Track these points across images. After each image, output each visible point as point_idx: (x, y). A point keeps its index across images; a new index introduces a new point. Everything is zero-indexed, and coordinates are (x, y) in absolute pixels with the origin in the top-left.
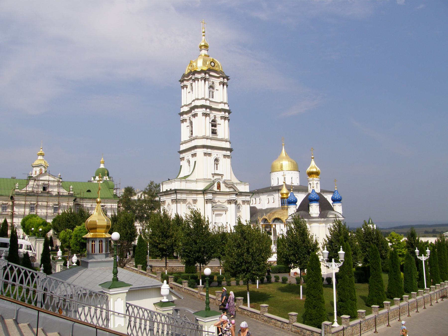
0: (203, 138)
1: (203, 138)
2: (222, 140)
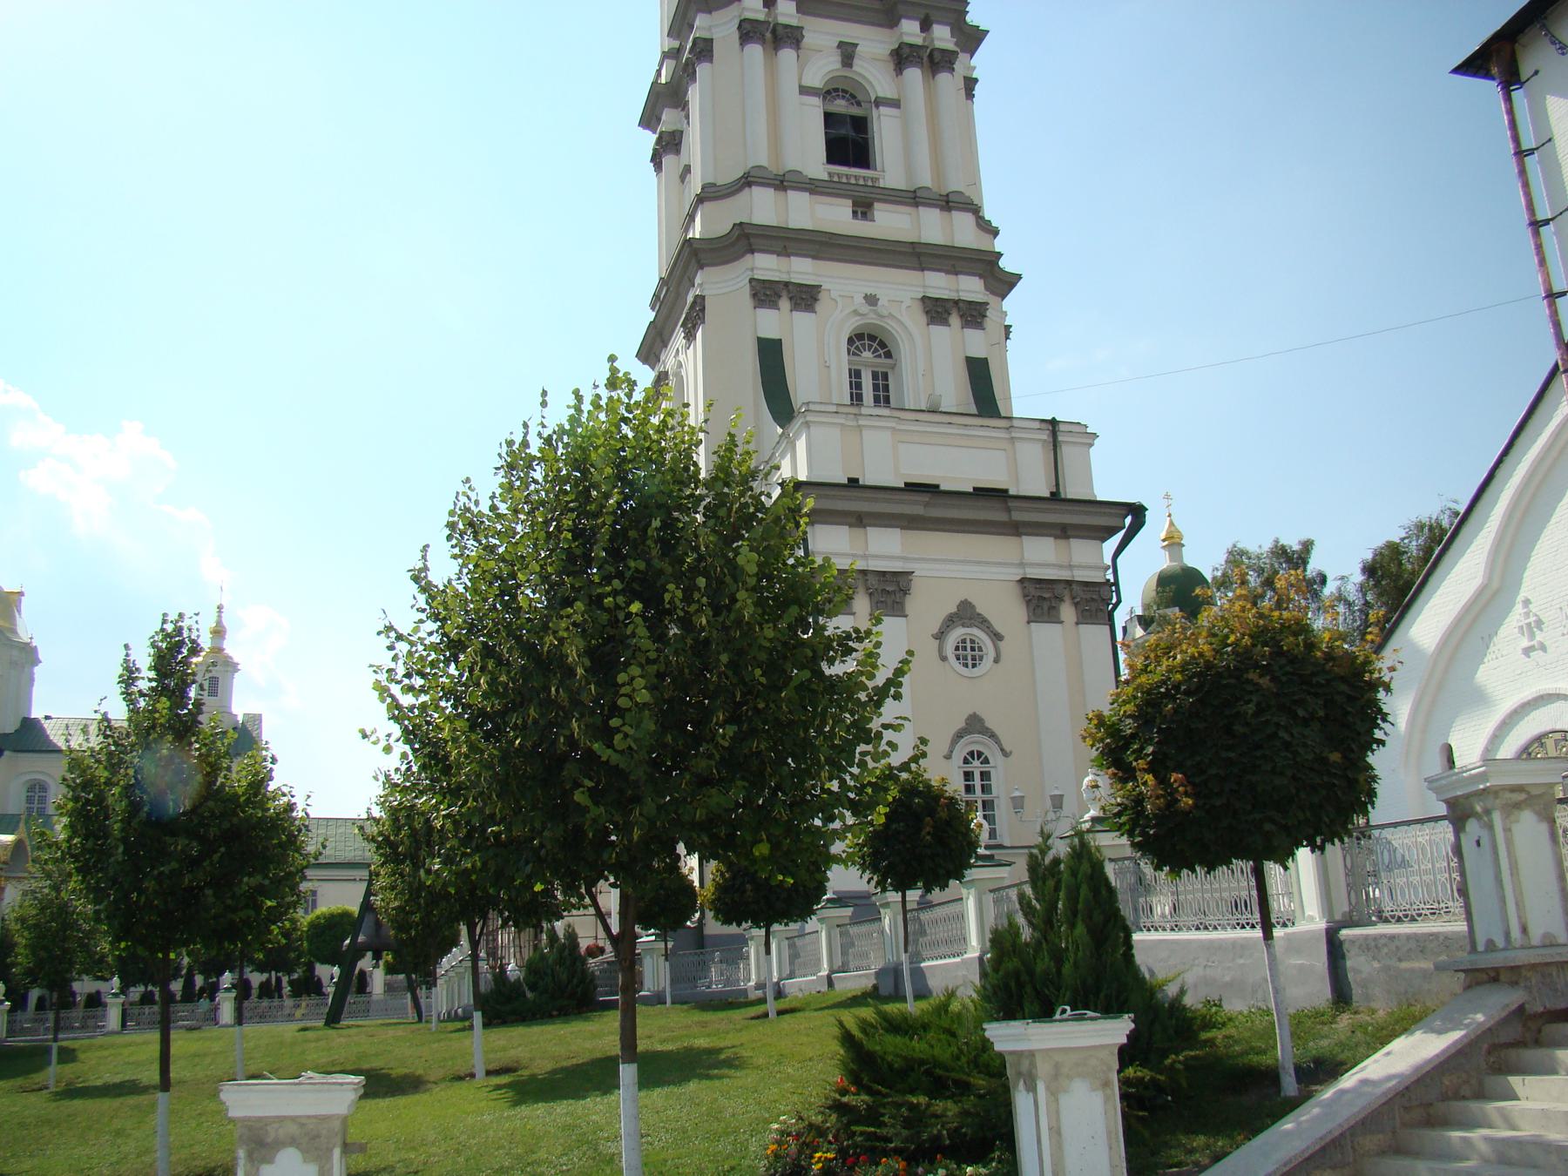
0: (748, 181)
1: (748, 181)
2: (914, 198)
